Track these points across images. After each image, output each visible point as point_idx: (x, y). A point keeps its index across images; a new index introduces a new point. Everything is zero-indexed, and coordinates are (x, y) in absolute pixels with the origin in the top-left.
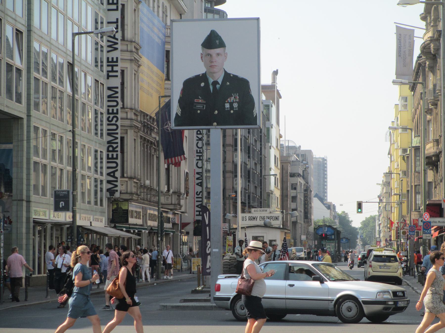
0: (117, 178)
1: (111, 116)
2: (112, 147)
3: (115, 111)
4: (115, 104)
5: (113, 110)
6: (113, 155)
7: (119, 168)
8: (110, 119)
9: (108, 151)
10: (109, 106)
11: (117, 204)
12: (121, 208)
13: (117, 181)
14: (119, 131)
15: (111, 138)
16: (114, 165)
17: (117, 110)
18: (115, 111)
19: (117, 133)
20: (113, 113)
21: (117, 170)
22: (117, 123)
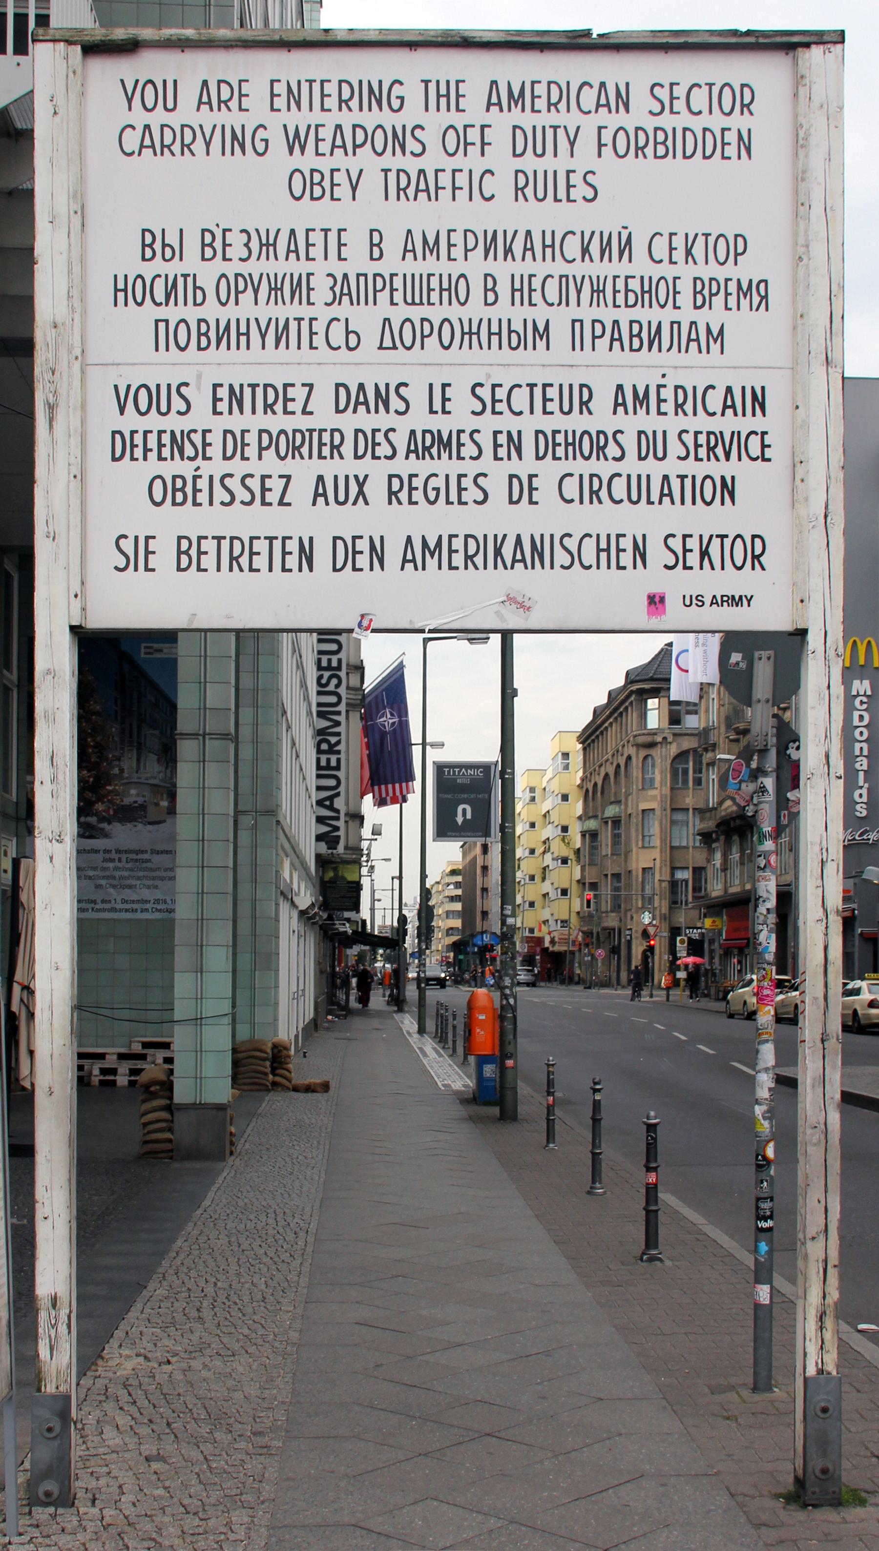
0: (338, 811)
1: (327, 674)
2: (328, 742)
3: (334, 664)
4: (334, 647)
5: (330, 661)
6: (328, 760)
7: (342, 789)
8: (324, 681)
9: (319, 751)
10: (320, 652)
11: (335, 870)
12: (344, 878)
13: (337, 819)
14: (342, 708)
15: (324, 724)
16: (332, 782)
17: (340, 661)
18: (334, 664)
19: (339, 713)
20: (329, 668)
21: (338, 794)
22: (338, 690)
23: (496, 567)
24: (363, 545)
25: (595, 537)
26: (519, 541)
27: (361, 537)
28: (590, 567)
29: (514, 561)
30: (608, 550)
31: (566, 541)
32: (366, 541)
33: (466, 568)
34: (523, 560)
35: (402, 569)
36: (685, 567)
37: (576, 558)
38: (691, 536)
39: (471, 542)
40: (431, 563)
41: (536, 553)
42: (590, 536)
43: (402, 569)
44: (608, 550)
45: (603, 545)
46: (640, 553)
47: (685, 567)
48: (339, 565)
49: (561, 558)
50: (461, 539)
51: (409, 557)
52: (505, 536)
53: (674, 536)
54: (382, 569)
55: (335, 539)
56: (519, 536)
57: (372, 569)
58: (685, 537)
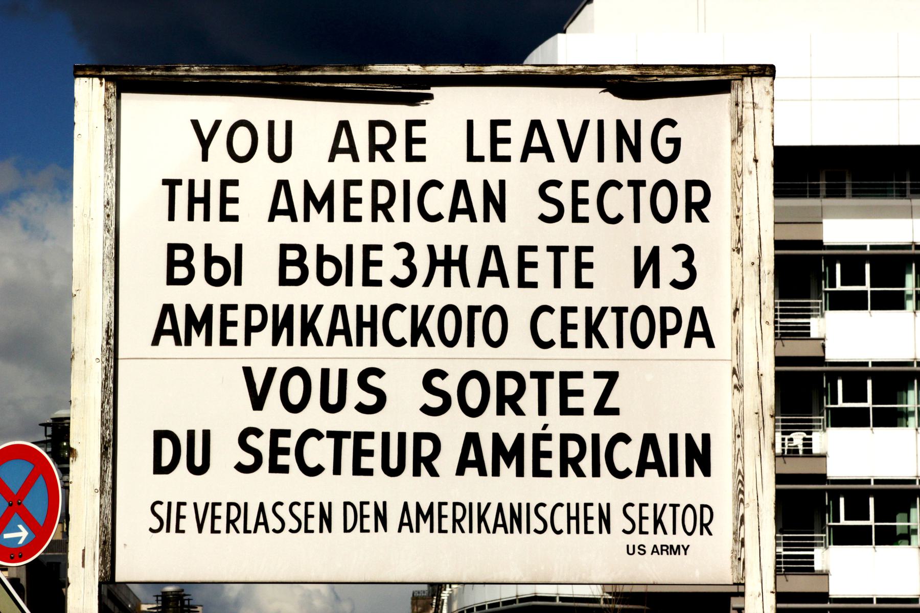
23: (479, 531)
24: (369, 510)
25: (565, 507)
26: (500, 508)
27: (368, 503)
28: (561, 532)
29: (496, 525)
30: (578, 518)
31: (541, 509)
32: (372, 506)
33: (454, 531)
34: (504, 525)
35: (400, 531)
36: (641, 532)
37: (549, 525)
38: (647, 505)
39: (459, 509)
40: (425, 526)
41: (514, 519)
42: (561, 505)
43: (400, 531)
44: (577, 518)
45: (573, 514)
46: (605, 520)
47: (641, 532)
48: (349, 527)
49: (536, 524)
50: (450, 506)
51: (406, 520)
52: (489, 504)
53: (632, 505)
54: (386, 530)
55: (346, 504)
56: (500, 505)
57: (376, 530)
58: (641, 505)
